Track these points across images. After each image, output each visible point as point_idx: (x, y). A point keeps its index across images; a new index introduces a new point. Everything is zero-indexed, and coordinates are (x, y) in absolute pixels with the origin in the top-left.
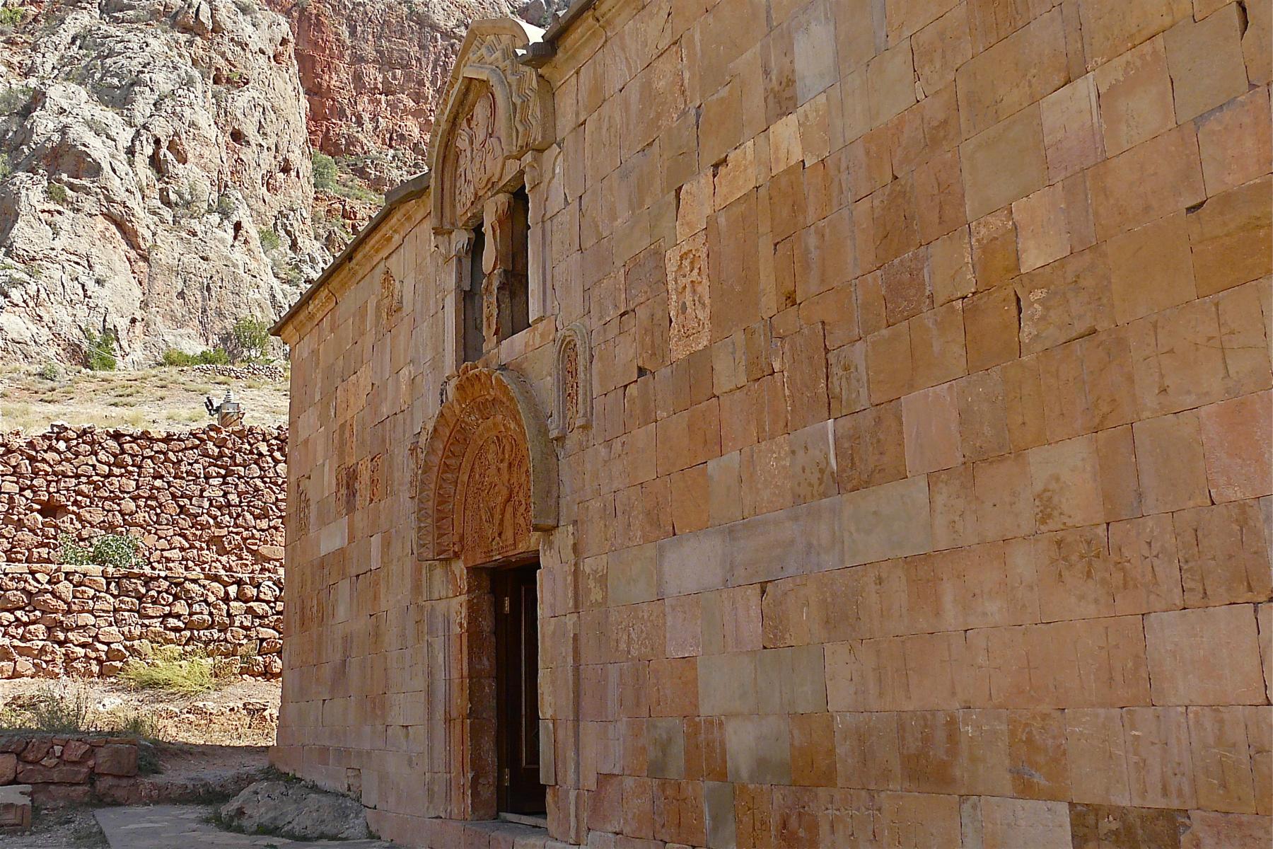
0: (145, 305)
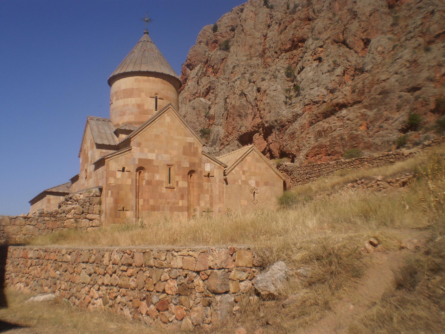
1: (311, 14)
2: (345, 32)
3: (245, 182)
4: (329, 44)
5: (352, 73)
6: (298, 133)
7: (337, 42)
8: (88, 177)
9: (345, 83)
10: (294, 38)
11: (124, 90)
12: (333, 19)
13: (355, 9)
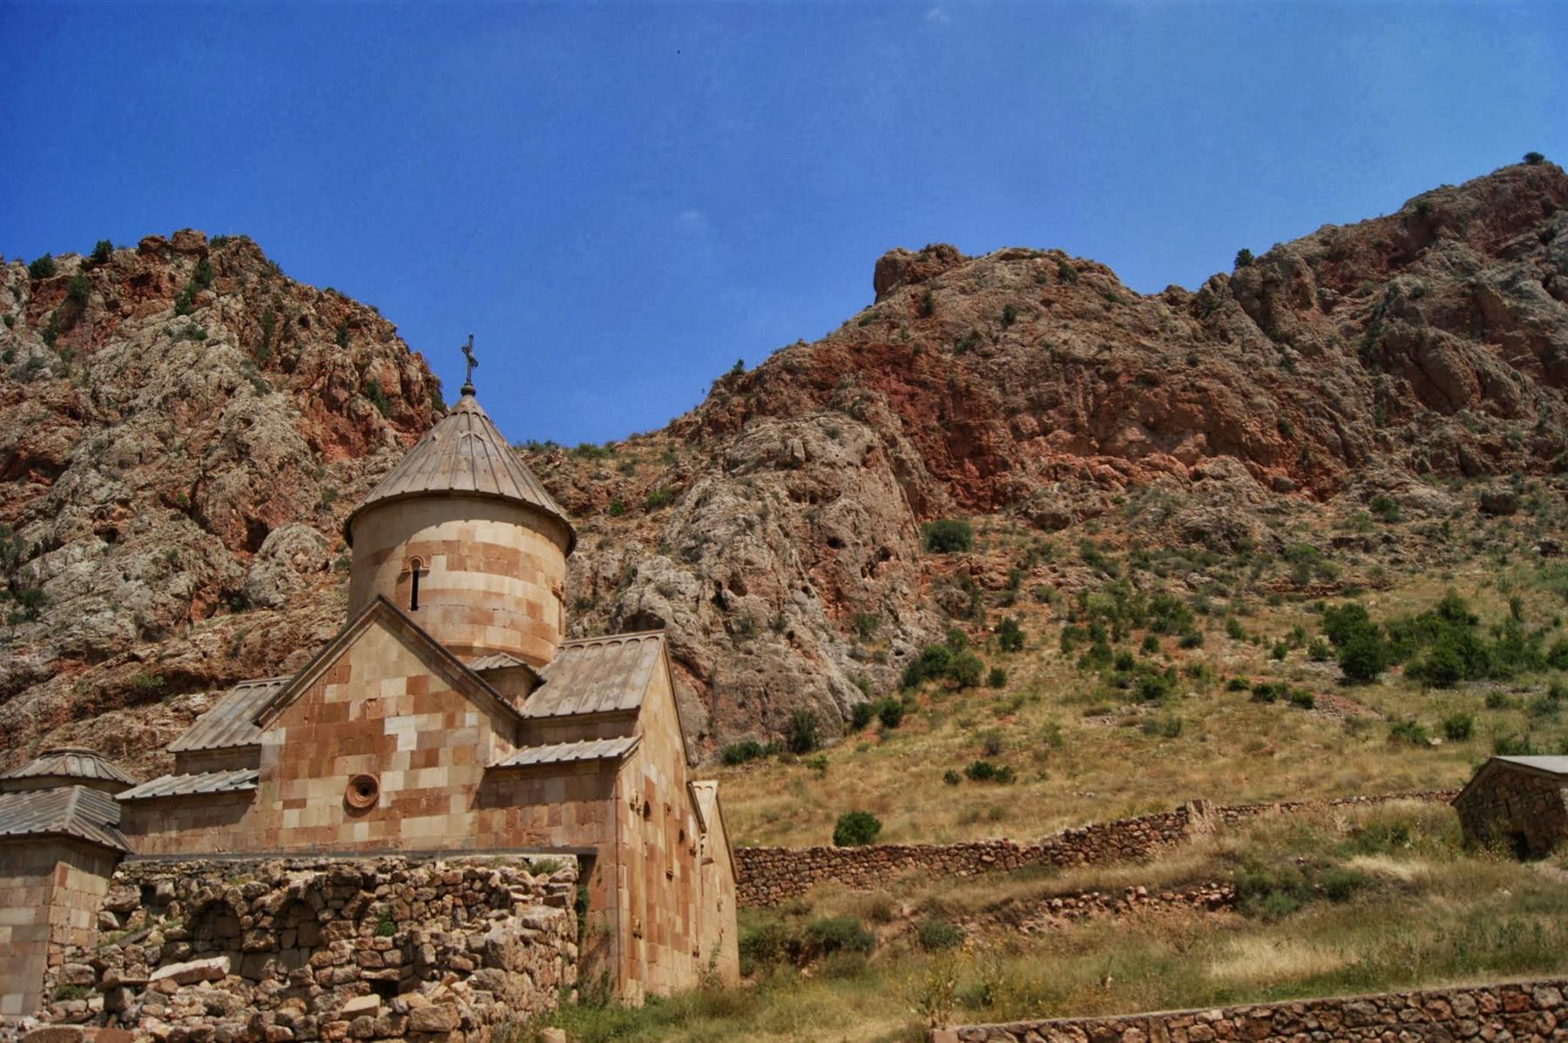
0: (711, 722)
1: (86, 402)
2: (201, 486)
3: (713, 875)
4: (146, 503)
5: (214, 598)
6: (30, 730)
7: (169, 505)
8: (383, 803)
9: (190, 621)
10: (22, 448)
11: (488, 547)
12: (170, 441)
13: (247, 436)
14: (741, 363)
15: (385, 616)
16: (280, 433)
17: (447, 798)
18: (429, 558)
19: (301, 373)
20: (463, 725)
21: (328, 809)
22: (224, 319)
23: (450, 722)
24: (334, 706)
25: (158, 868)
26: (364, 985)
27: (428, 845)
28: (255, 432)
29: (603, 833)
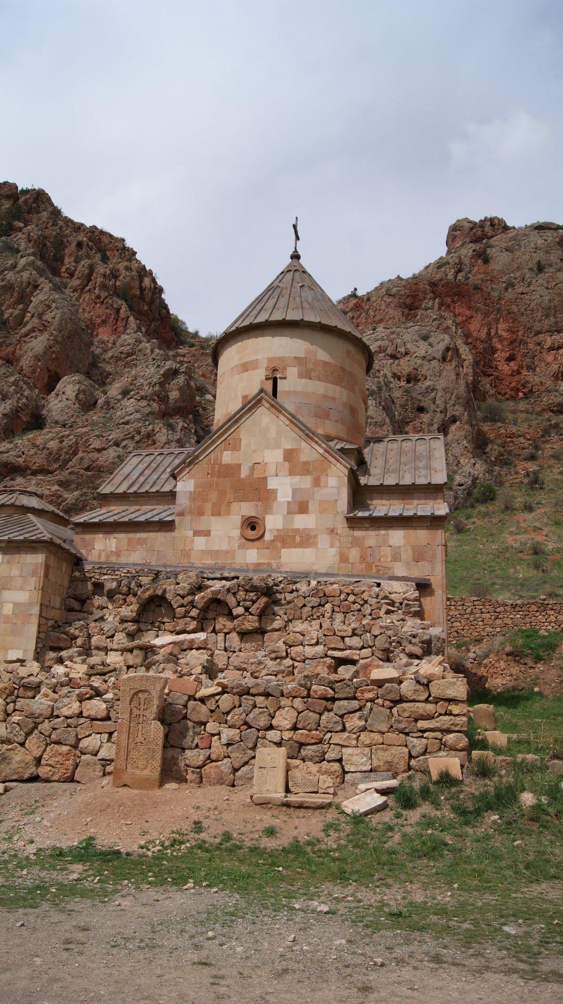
2: (18, 347)
8: (268, 537)
11: (325, 363)
14: (356, 289)
15: (267, 405)
16: (68, 315)
17: (316, 536)
18: (284, 369)
19: (78, 278)
20: (326, 486)
21: (227, 539)
22: (30, 241)
23: (317, 483)
24: (227, 466)
25: (105, 572)
26: (328, 660)
27: (302, 568)
28: (53, 313)
29: (433, 568)
